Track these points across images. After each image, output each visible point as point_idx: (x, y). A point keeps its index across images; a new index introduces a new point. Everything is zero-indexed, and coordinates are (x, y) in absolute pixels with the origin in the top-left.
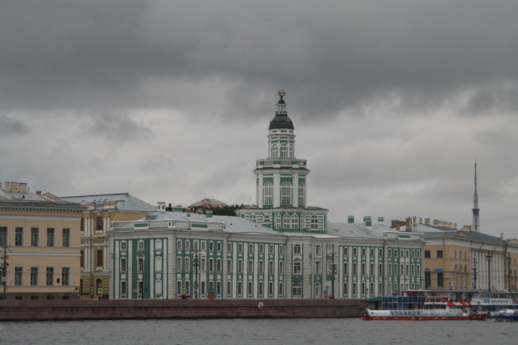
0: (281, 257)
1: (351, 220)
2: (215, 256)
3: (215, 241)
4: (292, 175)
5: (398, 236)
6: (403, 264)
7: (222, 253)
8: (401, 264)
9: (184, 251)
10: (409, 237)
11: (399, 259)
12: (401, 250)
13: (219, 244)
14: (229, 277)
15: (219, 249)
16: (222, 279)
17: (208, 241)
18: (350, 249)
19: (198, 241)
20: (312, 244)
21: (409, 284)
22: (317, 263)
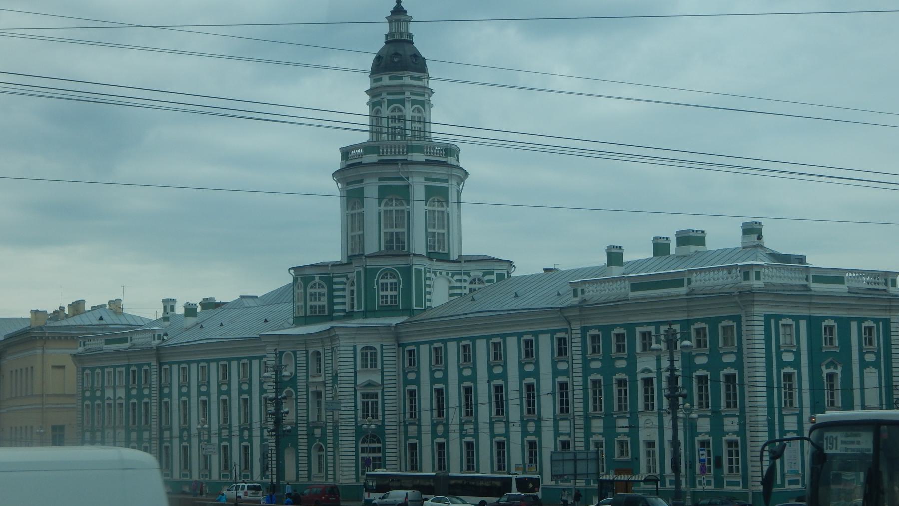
2: (140, 396)
3: (140, 366)
4: (408, 178)
5: (811, 279)
6: (653, 375)
8: (640, 376)
10: (679, 283)
11: (632, 361)
12: (639, 330)
13: (146, 371)
14: (500, 428)
17: (128, 367)
18: (452, 347)
19: (112, 369)
20: (295, 353)
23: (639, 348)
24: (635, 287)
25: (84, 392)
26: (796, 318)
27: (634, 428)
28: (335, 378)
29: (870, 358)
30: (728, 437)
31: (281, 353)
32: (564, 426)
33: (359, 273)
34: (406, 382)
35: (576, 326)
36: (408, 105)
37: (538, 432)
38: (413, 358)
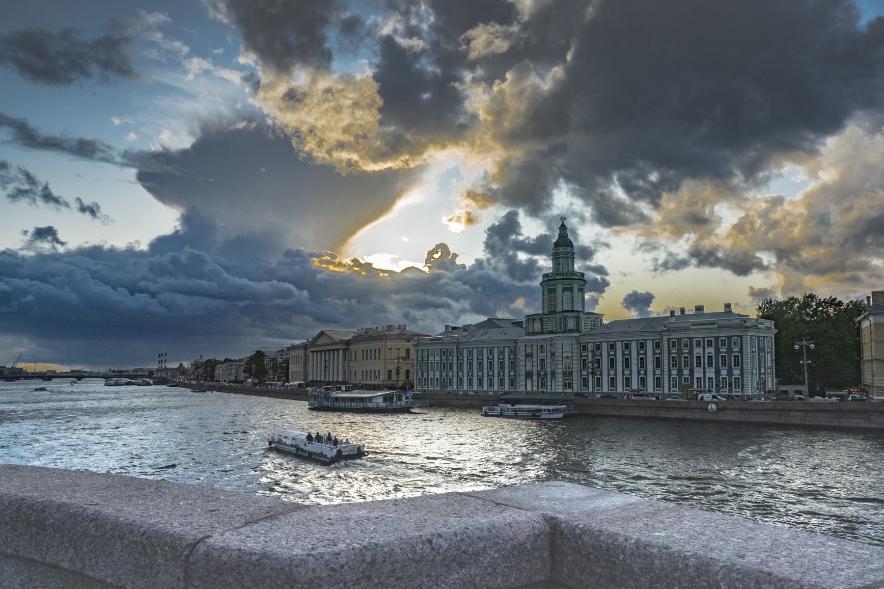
0: (512, 357)
1: (672, 313)
2: (447, 359)
3: (447, 349)
7: (453, 357)
8: (695, 356)
9: (422, 358)
10: (715, 324)
12: (694, 340)
13: (450, 351)
15: (450, 354)
16: (453, 376)
17: (441, 350)
20: (532, 346)
21: (713, 375)
22: (543, 360)
23: (694, 346)
24: (693, 325)
25: (417, 358)
26: (755, 336)
27: (692, 372)
28: (553, 354)
29: (769, 350)
30: (735, 376)
31: (526, 346)
32: (658, 372)
33: (560, 318)
34: (581, 356)
35: (665, 338)
36: (561, 259)
37: (646, 374)
38: (585, 348)
